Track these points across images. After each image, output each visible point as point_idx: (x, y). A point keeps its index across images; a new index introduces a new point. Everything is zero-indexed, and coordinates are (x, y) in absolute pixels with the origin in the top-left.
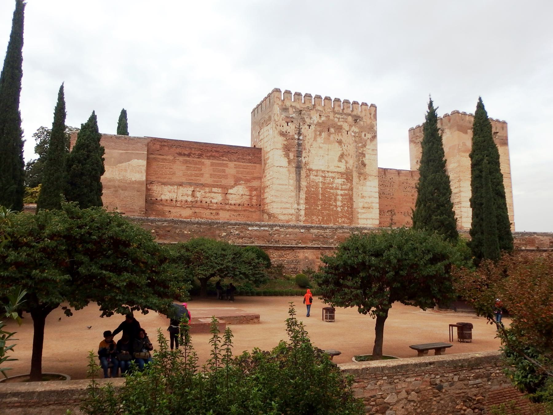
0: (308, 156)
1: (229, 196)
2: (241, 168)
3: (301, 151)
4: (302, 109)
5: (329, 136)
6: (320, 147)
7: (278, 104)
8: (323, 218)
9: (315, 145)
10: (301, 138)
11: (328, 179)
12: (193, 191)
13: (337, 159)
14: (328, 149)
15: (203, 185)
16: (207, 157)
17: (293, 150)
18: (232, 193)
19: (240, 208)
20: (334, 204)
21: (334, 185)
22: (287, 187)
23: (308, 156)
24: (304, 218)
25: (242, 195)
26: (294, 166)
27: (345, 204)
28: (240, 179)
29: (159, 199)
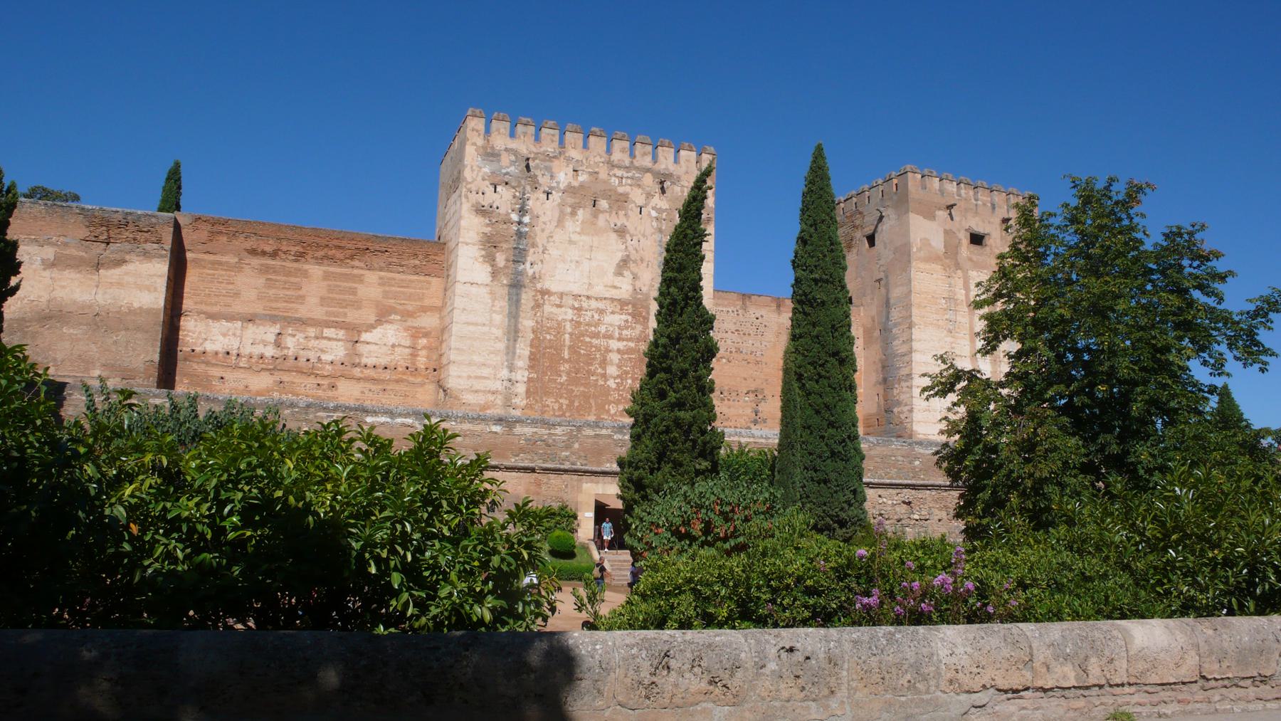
0: (542, 261)
1: (361, 348)
2: (393, 286)
3: (524, 250)
4: (532, 156)
5: (595, 216)
6: (571, 242)
7: (474, 144)
8: (572, 402)
9: (559, 236)
10: (526, 219)
11: (588, 313)
12: (279, 334)
13: (611, 269)
14: (592, 247)
15: (304, 323)
16: (317, 258)
17: (505, 246)
18: (369, 340)
19: (387, 375)
20: (600, 370)
21: (602, 329)
22: (486, 329)
23: (542, 261)
24: (525, 402)
25: (393, 346)
26: (505, 282)
27: (627, 373)
28: (392, 310)
29: (198, 349)
